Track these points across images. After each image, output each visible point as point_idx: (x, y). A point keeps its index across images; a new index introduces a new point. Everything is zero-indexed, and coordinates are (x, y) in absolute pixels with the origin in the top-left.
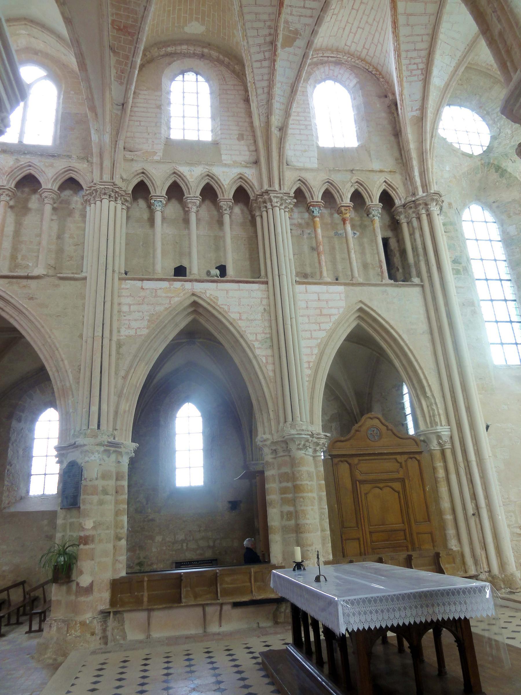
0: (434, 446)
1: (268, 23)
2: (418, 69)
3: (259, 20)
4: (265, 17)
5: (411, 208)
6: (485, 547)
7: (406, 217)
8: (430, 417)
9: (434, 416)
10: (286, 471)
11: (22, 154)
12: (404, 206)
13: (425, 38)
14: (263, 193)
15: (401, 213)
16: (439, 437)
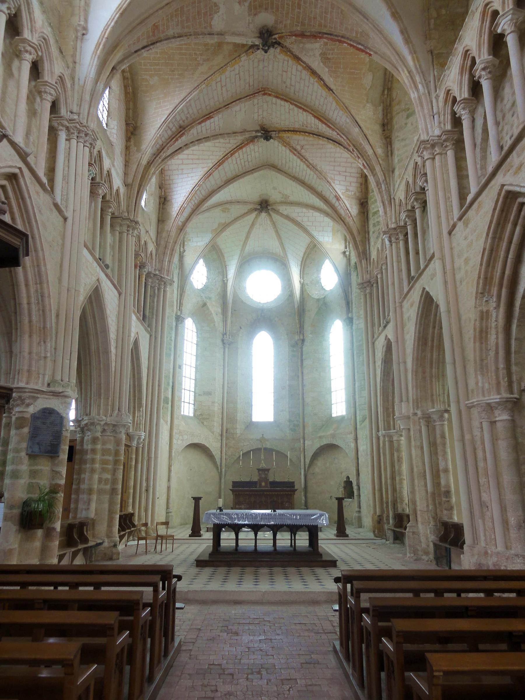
0: (134, 444)
1: (188, 116)
2: (194, 201)
3: (188, 109)
4: (191, 112)
5: (158, 279)
6: (146, 510)
7: (152, 282)
8: (137, 424)
9: (140, 424)
10: (110, 447)
11: (48, 22)
12: (155, 275)
13: (207, 191)
14: (134, 221)
15: (151, 277)
16: (139, 438)
